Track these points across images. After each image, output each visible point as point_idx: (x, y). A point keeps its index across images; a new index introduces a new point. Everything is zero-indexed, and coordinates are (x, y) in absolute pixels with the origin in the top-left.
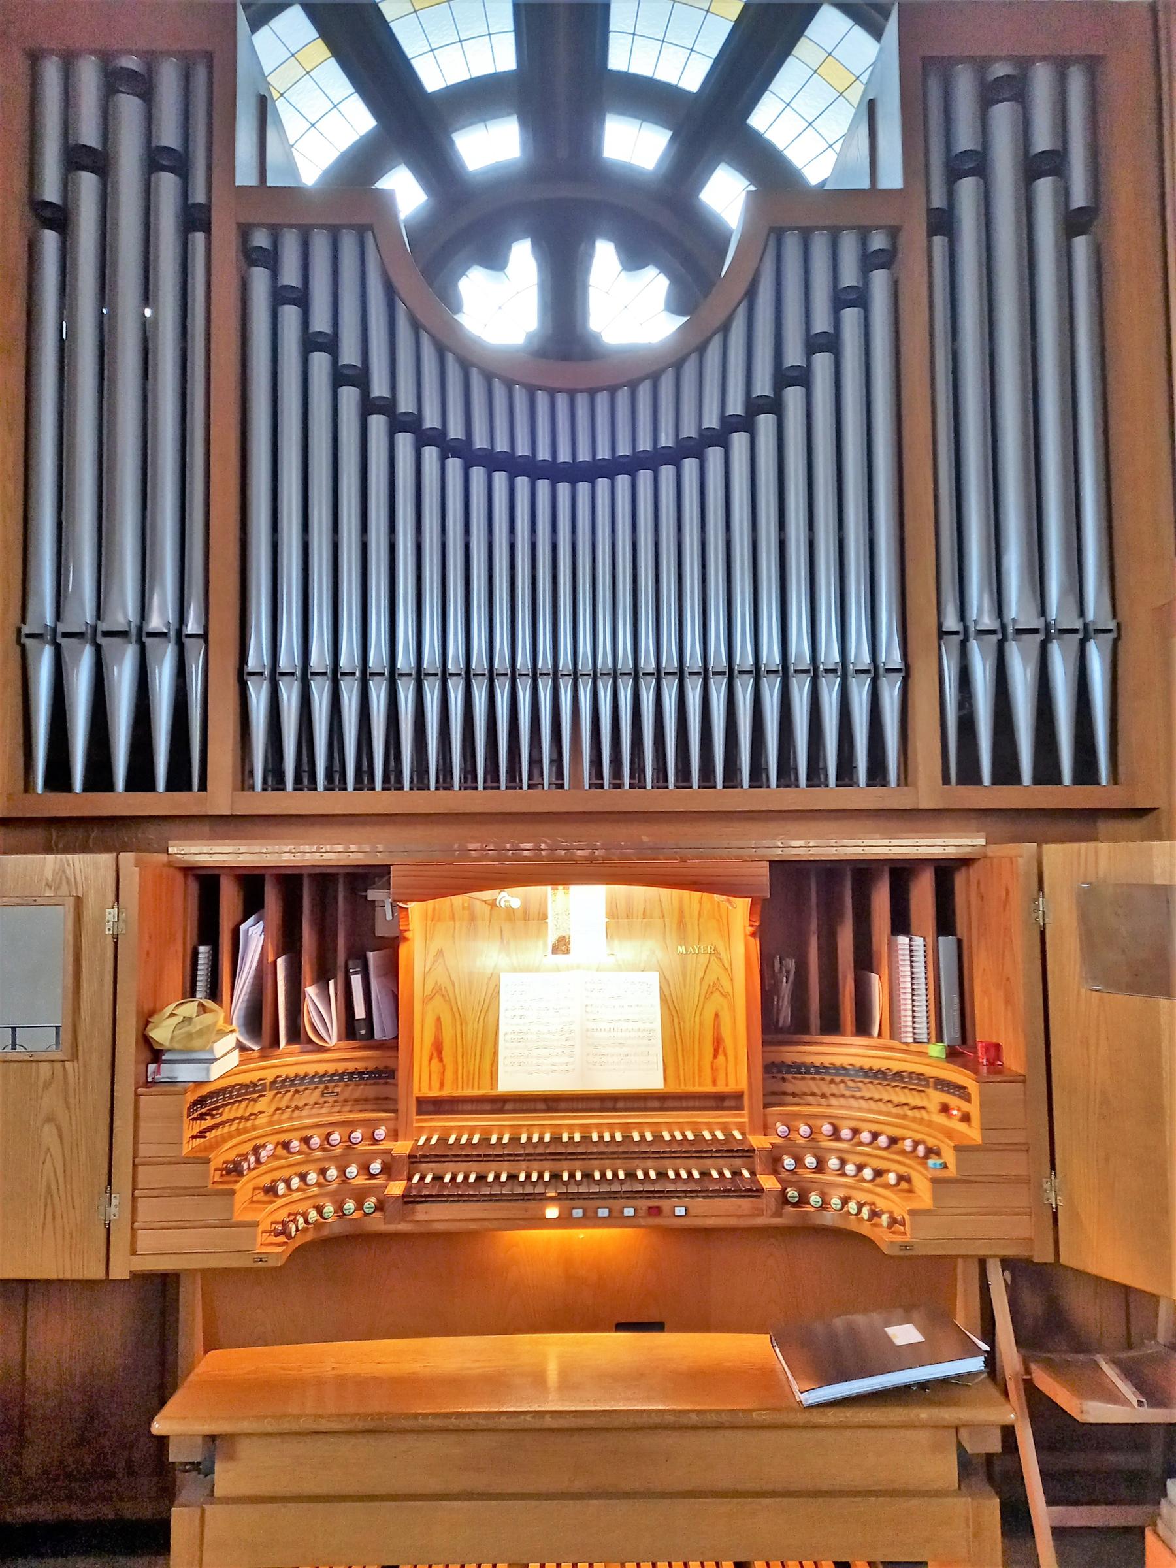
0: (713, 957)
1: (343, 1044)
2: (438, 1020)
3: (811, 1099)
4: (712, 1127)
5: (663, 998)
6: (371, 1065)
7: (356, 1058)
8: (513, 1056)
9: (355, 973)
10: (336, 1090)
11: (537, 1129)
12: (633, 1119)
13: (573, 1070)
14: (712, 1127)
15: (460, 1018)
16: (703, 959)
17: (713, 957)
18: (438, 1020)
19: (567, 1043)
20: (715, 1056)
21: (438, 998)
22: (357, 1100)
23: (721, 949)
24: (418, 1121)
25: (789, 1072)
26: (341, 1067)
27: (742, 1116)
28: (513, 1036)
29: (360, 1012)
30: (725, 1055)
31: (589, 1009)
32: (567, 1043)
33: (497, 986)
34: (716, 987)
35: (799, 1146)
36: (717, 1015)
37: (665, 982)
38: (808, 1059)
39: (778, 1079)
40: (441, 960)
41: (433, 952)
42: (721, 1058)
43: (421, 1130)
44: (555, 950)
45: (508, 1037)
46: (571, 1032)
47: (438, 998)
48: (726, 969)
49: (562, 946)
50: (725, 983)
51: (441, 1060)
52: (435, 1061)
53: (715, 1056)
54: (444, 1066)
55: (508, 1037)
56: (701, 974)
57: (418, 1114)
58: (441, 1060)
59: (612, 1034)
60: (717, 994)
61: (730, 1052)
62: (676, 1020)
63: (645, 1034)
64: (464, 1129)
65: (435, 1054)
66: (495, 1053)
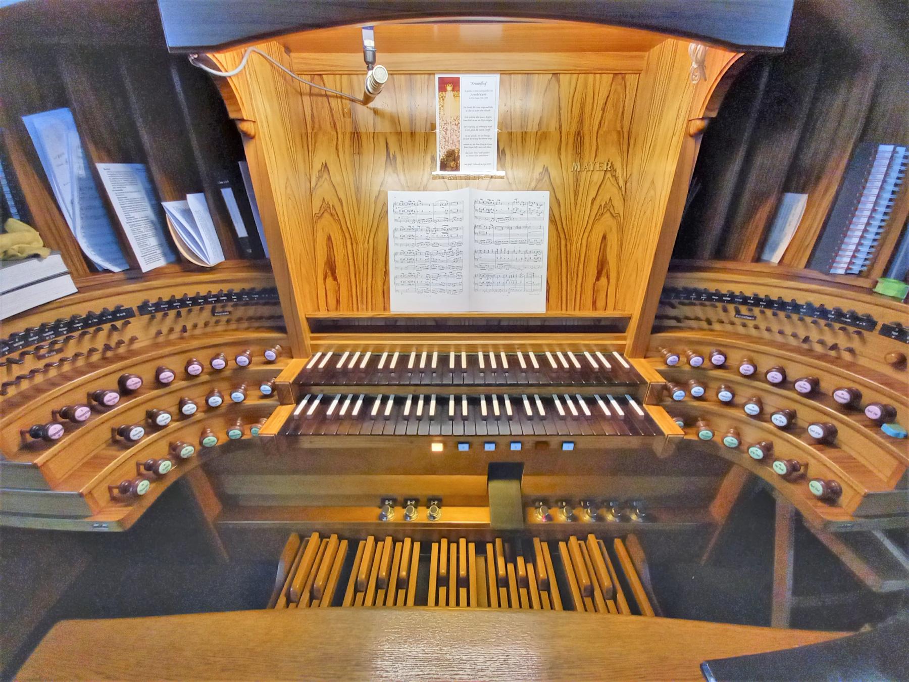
0: (609, 175)
1: (231, 263)
2: (329, 238)
3: (693, 324)
4: (595, 352)
5: (553, 220)
6: (258, 286)
7: (241, 279)
8: (403, 276)
9: (224, 186)
10: (229, 309)
11: (424, 351)
12: (516, 340)
13: (461, 291)
14: (595, 352)
15: (350, 237)
16: (597, 177)
17: (609, 175)
18: (329, 238)
19: (455, 264)
20: (598, 279)
21: (326, 214)
22: (250, 319)
23: (618, 166)
24: (312, 339)
25: (677, 297)
26: (225, 288)
27: (625, 339)
28: (404, 257)
29: (241, 231)
30: (608, 277)
31: (477, 230)
32: (455, 264)
33: (385, 205)
34: (608, 207)
35: (683, 372)
36: (604, 237)
37: (556, 202)
38: (701, 286)
39: (670, 304)
40: (326, 176)
41: (317, 166)
42: (603, 280)
43: (315, 348)
44: (444, 166)
45: (398, 258)
46: (459, 253)
48: (620, 188)
49: (451, 161)
50: (618, 204)
51: (335, 279)
52: (330, 280)
53: (598, 279)
54: (338, 285)
55: (398, 258)
56: (592, 194)
57: (312, 332)
58: (335, 279)
59: (499, 256)
60: (608, 215)
61: (613, 275)
62: (563, 242)
63: (532, 256)
64: (354, 352)
65: (329, 273)
66: (386, 273)
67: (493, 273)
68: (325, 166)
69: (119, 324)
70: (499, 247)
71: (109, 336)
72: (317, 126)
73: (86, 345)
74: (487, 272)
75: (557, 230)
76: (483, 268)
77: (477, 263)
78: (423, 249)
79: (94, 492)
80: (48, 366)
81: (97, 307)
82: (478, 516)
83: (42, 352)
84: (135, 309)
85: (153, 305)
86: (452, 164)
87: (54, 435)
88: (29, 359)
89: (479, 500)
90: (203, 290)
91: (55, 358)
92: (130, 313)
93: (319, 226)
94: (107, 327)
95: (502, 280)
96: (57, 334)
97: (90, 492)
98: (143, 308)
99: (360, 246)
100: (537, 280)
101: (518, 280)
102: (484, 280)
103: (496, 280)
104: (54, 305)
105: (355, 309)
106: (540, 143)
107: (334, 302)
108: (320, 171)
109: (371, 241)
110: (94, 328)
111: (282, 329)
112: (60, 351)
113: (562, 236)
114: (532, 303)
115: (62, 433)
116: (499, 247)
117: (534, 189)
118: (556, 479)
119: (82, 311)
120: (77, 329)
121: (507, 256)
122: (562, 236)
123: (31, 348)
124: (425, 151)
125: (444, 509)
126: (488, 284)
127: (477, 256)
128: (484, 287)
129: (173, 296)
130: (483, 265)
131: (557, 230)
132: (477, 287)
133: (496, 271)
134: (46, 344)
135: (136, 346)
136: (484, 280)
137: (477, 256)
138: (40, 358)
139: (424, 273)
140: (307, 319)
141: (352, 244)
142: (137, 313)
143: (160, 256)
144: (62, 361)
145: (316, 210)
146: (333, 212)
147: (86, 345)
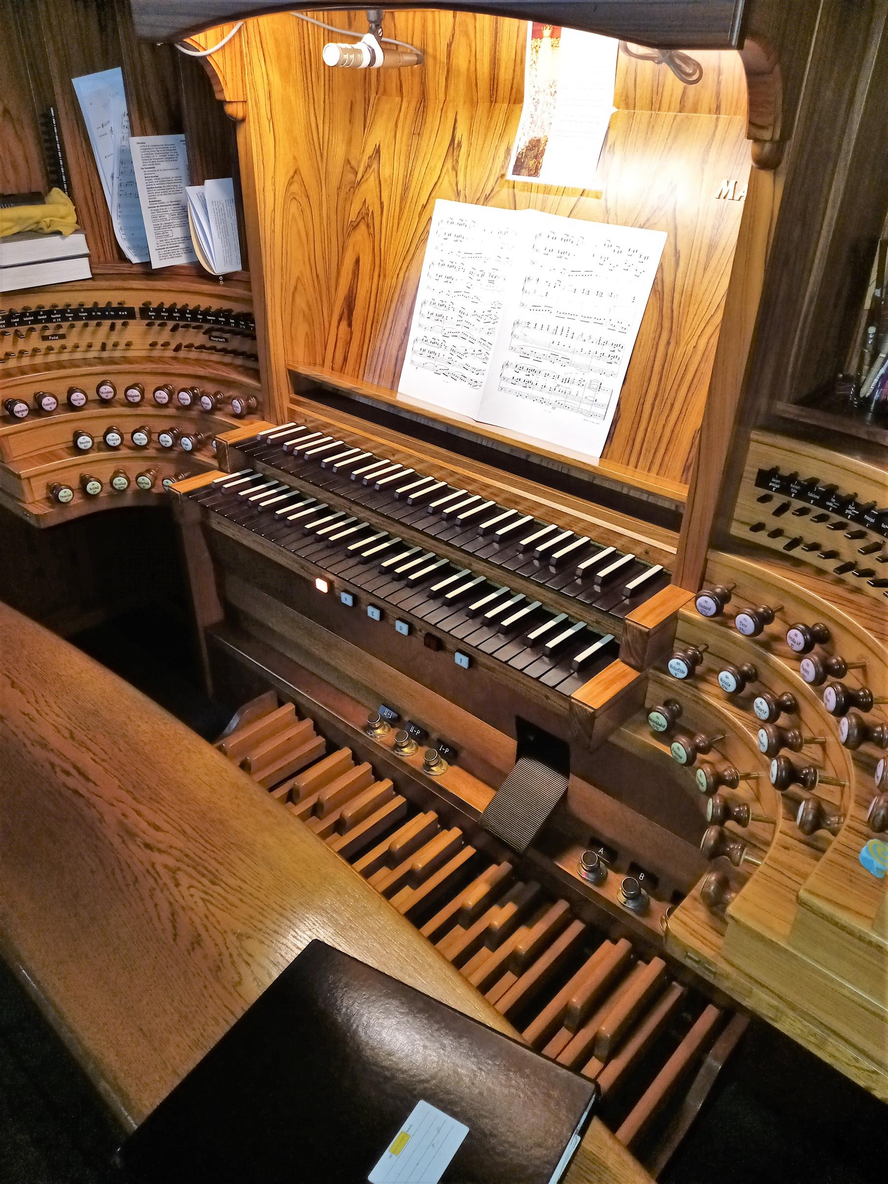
2: (357, 261)
5: (658, 290)
18: (357, 261)
24: (293, 401)
26: (226, 305)
37: (673, 256)
45: (428, 308)
47: (363, 226)
51: (350, 325)
52: (344, 324)
54: (351, 333)
55: (428, 308)
58: (350, 325)
59: (557, 338)
63: (607, 350)
64: (324, 431)
65: (346, 314)
66: (407, 331)
67: (538, 366)
68: (378, 151)
69: (119, 323)
70: (565, 323)
71: (108, 336)
72: (381, 89)
73: (87, 339)
74: (530, 363)
75: (661, 310)
76: (525, 356)
77: (516, 343)
78: (459, 303)
79: (32, 480)
80: (50, 349)
81: (103, 298)
82: (476, 795)
83: (48, 333)
84: (137, 310)
85: (155, 310)
86: (532, 163)
87: (18, 412)
88: (35, 335)
89: (492, 777)
90: (204, 303)
91: (57, 344)
92: (131, 314)
93: (352, 240)
94: (107, 323)
95: (550, 383)
96: (65, 319)
97: (28, 478)
98: (145, 311)
99: (388, 280)
100: (603, 397)
101: (574, 389)
102: (522, 375)
103: (541, 380)
104: (64, 288)
105: (360, 377)
106: (675, 137)
107: (342, 358)
108: (370, 157)
109: (401, 275)
110: (95, 322)
111: (256, 374)
112: (63, 337)
113: (666, 324)
114: (577, 434)
115: (25, 413)
116: (565, 323)
117: (641, 227)
118: (629, 815)
119: (89, 299)
120: (81, 318)
121: (567, 341)
122: (666, 324)
123: (38, 327)
124: (501, 136)
125: (455, 768)
126: (527, 384)
127: (518, 331)
128: (519, 388)
129: (175, 304)
130: (527, 350)
131: (661, 310)
132: (504, 384)
133: (545, 366)
134: (51, 326)
135: (130, 354)
136: (522, 375)
137: (518, 331)
138: (45, 338)
139: (450, 342)
140: (290, 371)
141: (379, 276)
142: (138, 315)
143: (181, 251)
144: (64, 347)
145: (353, 217)
146: (370, 222)
147: (87, 339)
